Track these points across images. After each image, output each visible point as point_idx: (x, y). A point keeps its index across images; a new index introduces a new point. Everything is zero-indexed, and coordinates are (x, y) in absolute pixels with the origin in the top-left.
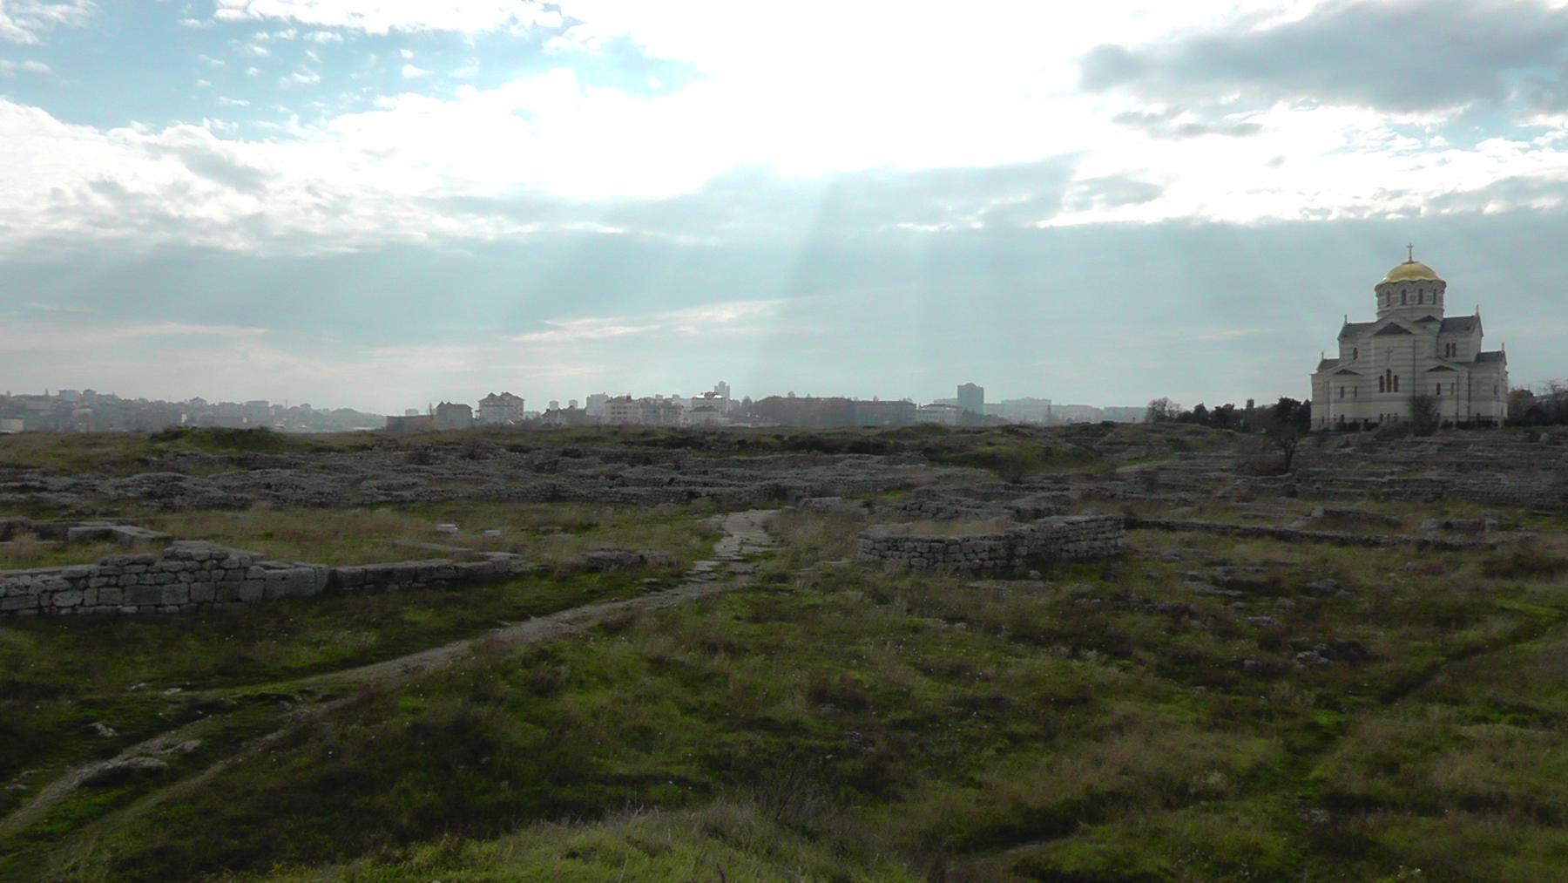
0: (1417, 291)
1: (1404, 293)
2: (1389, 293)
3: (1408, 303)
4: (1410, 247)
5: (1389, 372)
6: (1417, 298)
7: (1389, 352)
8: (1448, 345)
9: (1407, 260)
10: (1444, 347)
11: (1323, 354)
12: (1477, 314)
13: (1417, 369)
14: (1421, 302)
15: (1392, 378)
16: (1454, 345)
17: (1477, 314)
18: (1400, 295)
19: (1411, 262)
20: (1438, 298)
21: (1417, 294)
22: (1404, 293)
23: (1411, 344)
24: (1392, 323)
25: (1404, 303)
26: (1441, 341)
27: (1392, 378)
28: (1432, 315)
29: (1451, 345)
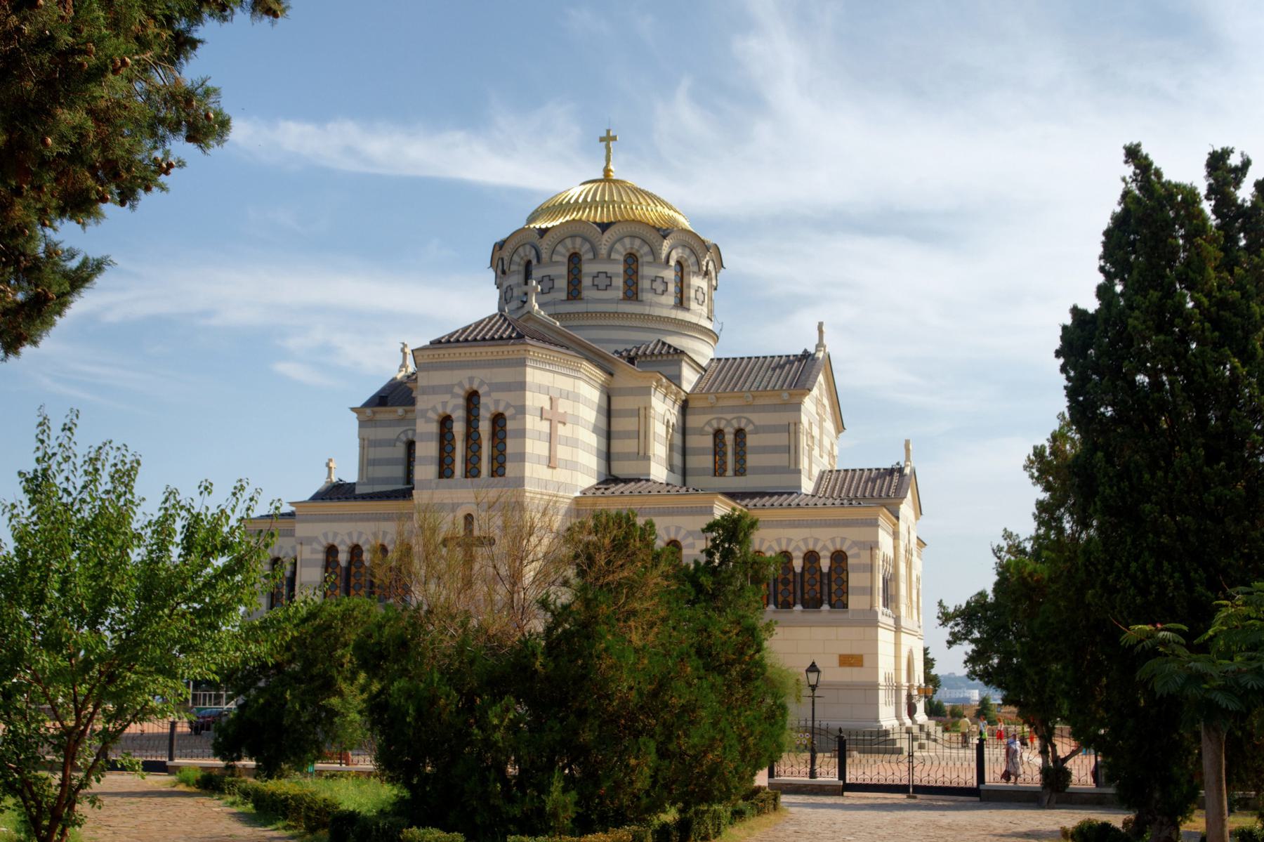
1: (574, 259)
3: (586, 294)
4: (608, 139)
6: (619, 282)
8: (718, 434)
9: (600, 176)
10: (708, 442)
12: (820, 345)
16: (740, 433)
17: (820, 345)
18: (563, 270)
19: (607, 178)
22: (574, 259)
25: (574, 292)
26: (694, 421)
29: (729, 439)
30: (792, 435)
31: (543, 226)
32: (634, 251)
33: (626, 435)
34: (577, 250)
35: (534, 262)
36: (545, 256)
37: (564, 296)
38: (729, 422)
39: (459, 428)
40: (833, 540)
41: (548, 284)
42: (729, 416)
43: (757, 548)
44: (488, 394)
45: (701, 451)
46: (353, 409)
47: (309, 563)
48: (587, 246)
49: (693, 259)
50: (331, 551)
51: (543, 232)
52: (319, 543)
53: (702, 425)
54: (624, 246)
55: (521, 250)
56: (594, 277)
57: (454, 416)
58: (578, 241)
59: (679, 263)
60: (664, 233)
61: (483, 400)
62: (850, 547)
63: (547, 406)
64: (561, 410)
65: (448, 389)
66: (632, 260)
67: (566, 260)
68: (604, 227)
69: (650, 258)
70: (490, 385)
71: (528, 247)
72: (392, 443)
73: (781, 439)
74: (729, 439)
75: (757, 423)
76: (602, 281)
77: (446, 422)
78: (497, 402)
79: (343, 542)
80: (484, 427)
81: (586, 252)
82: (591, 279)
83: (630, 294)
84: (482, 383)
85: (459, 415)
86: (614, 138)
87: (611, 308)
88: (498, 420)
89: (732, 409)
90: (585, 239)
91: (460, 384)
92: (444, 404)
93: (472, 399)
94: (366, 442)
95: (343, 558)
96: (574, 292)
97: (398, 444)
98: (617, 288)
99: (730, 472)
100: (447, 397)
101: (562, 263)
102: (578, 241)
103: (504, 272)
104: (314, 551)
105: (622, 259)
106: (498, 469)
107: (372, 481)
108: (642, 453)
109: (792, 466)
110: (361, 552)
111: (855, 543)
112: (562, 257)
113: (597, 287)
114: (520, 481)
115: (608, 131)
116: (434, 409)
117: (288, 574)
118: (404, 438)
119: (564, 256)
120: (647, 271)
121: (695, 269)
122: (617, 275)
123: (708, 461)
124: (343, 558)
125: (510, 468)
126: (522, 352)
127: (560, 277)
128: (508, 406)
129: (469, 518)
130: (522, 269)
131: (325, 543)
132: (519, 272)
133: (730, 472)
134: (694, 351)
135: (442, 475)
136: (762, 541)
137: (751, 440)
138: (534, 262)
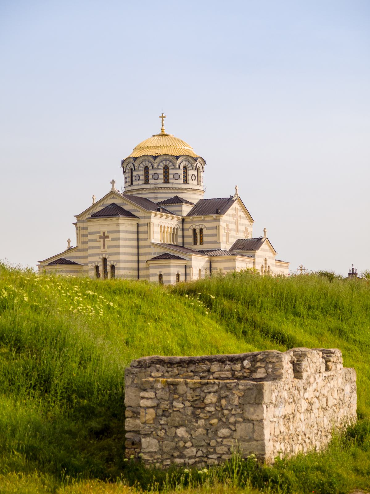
0: (161, 167)
3: (151, 181)
4: (162, 117)
5: (105, 260)
6: (162, 176)
7: (104, 237)
8: (194, 230)
9: (159, 132)
10: (191, 233)
12: (236, 194)
13: (141, 258)
15: (109, 268)
16: (201, 230)
17: (236, 194)
21: (161, 172)
22: (146, 168)
23: (135, 229)
24: (113, 204)
25: (147, 181)
26: (187, 226)
27: (109, 268)
28: (180, 196)
29: (198, 231)
35: (133, 170)
37: (143, 182)
41: (137, 178)
42: (197, 224)
45: (189, 237)
46: (74, 224)
48: (150, 164)
49: (190, 165)
55: (129, 164)
58: (147, 162)
60: (177, 157)
66: (166, 168)
67: (143, 169)
68: (155, 157)
69: (172, 167)
71: (131, 164)
73: (214, 232)
76: (156, 176)
81: (150, 167)
83: (166, 180)
86: (165, 117)
87: (159, 186)
89: (199, 222)
96: (147, 181)
98: (161, 179)
101: (142, 170)
102: (147, 162)
109: (218, 241)
112: (142, 168)
113: (154, 178)
115: (162, 114)
120: (171, 172)
121: (191, 168)
122: (161, 174)
123: (191, 240)
127: (142, 175)
130: (130, 171)
133: (198, 243)
134: (191, 198)
137: (205, 232)
138: (133, 170)
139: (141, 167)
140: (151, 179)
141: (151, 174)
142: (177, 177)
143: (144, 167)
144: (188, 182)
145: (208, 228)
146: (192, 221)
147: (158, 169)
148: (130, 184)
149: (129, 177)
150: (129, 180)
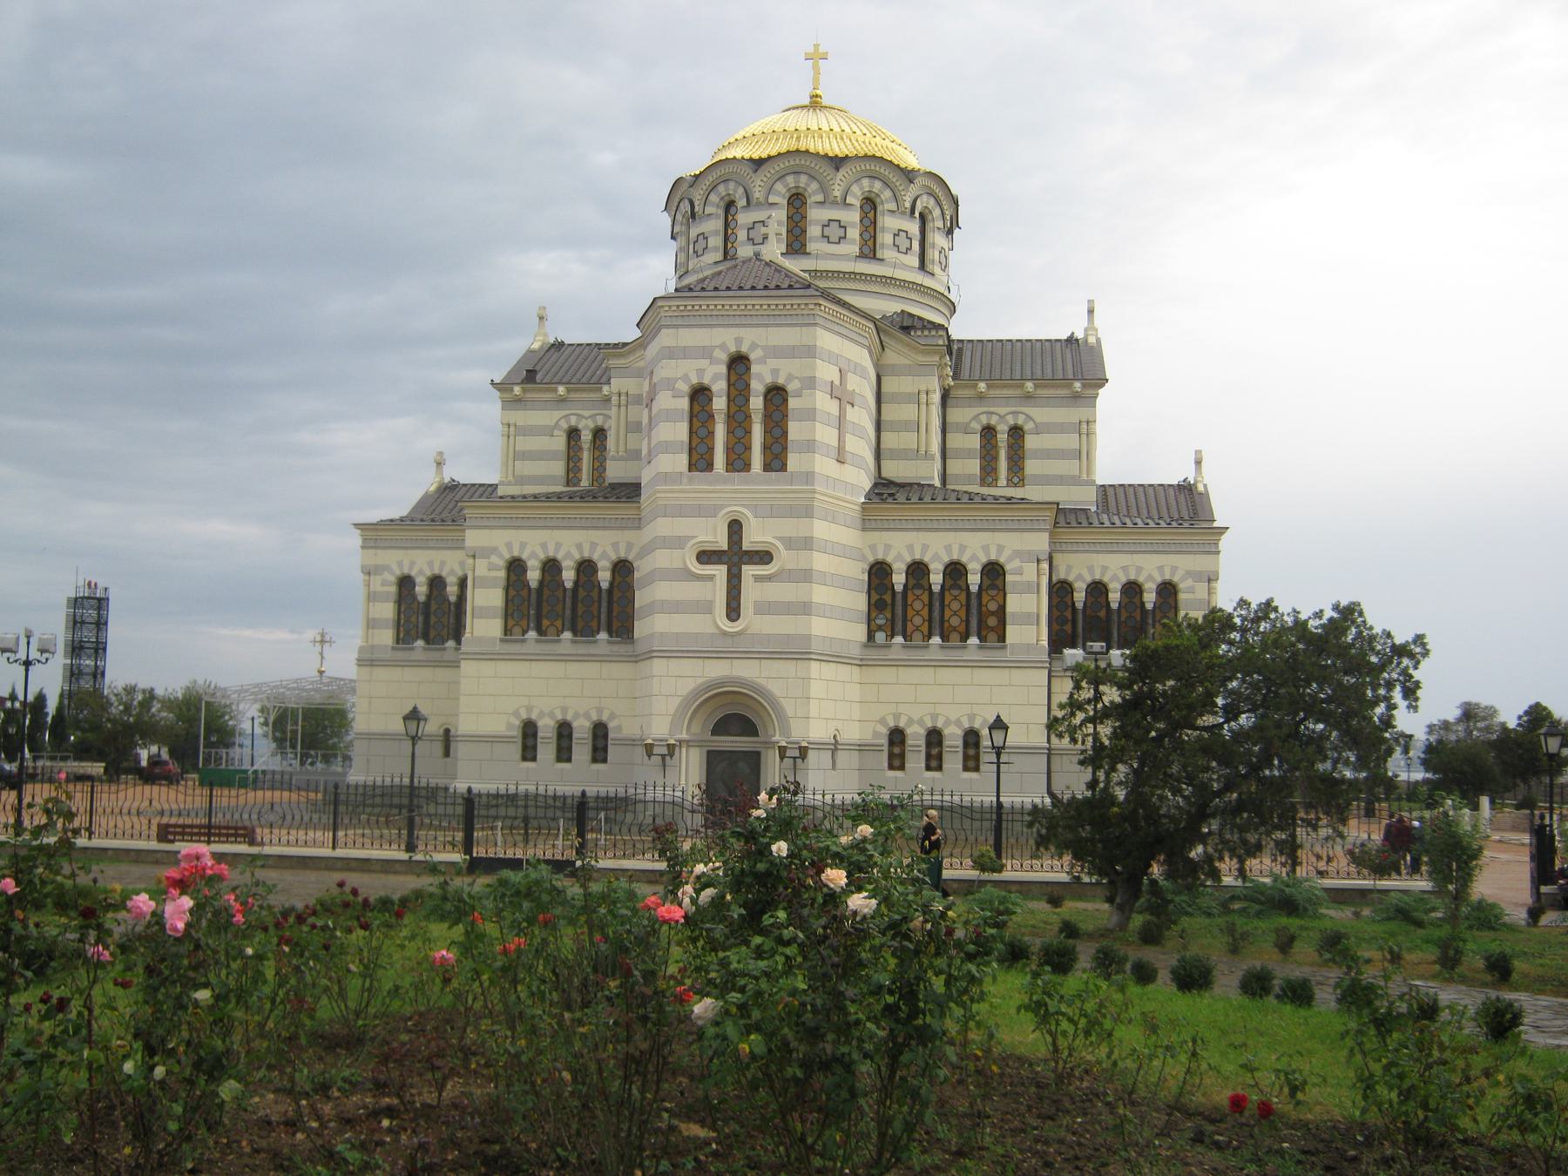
0: (854, 200)
1: (797, 201)
2: (729, 206)
6: (854, 233)
8: (988, 432)
9: (807, 101)
10: (974, 442)
11: (439, 464)
14: (870, 250)
16: (1016, 432)
18: (780, 215)
20: (933, 254)
21: (853, 217)
22: (797, 201)
26: (957, 415)
29: (1002, 438)
30: (1084, 437)
31: (755, 156)
32: (873, 195)
33: (904, 426)
34: (801, 191)
35: (742, 202)
36: (758, 194)
38: (1002, 417)
39: (719, 404)
40: (1160, 569)
42: (1002, 411)
43: (1062, 576)
44: (762, 361)
45: (966, 454)
47: (486, 583)
49: (937, 212)
50: (516, 567)
51: (758, 163)
52: (501, 556)
53: (967, 421)
54: (861, 188)
55: (721, 189)
56: (824, 226)
57: (714, 388)
58: (803, 179)
59: (921, 215)
61: (754, 369)
62: (1183, 579)
63: (837, 382)
64: (850, 388)
65: (706, 352)
68: (837, 162)
69: (893, 206)
70: (764, 348)
72: (548, 432)
73: (1070, 441)
74: (1002, 438)
75: (1038, 419)
76: (834, 231)
77: (700, 394)
78: (775, 372)
79: (533, 555)
80: (756, 403)
81: (814, 193)
82: (820, 228)
83: (866, 250)
84: (754, 346)
85: (719, 386)
88: (776, 395)
90: (813, 177)
91: (723, 347)
92: (700, 372)
93: (738, 363)
94: (512, 429)
95: (533, 576)
97: (556, 432)
99: (1003, 481)
100: (704, 363)
103: (693, 215)
104: (491, 567)
105: (858, 204)
106: (776, 459)
107: (521, 480)
108: (923, 449)
109: (1084, 476)
110: (559, 570)
111: (1189, 573)
112: (780, 197)
113: (827, 238)
114: (809, 477)
115: (816, 46)
116: (686, 378)
117: (453, 599)
118: (564, 425)
119: (784, 196)
120: (889, 223)
121: (939, 224)
122: (853, 225)
123: (974, 467)
124: (533, 576)
125: (793, 461)
126: (812, 307)
128: (790, 378)
129: (735, 528)
130: (721, 212)
131: (507, 556)
132: (717, 216)
133: (1003, 481)
135: (692, 467)
136: (1069, 568)
137: (1031, 442)
138: (742, 202)
139: (778, 194)
140: (816, 239)
141: (816, 222)
142: (903, 242)
143: (788, 195)
144: (929, 267)
145: (1038, 431)
146: (981, 397)
147: (845, 204)
148: (719, 256)
149: (716, 233)
150: (716, 241)
